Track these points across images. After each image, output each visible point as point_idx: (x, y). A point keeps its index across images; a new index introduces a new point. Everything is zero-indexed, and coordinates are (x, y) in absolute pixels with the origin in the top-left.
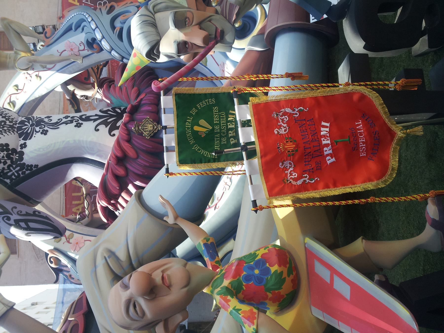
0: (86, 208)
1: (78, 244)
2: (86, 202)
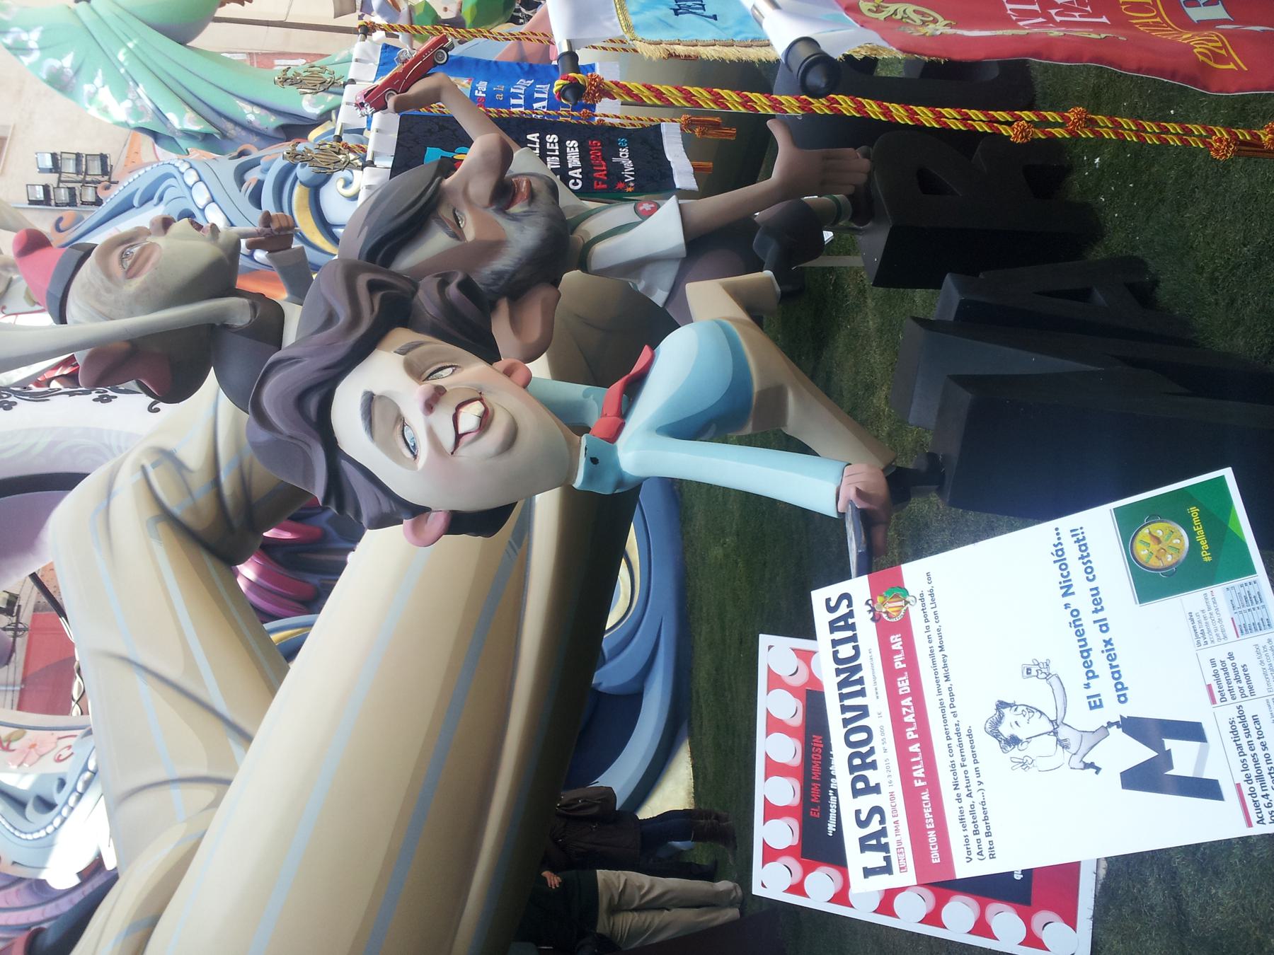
0: (74, 700)
1: (37, 747)
2: (79, 683)
